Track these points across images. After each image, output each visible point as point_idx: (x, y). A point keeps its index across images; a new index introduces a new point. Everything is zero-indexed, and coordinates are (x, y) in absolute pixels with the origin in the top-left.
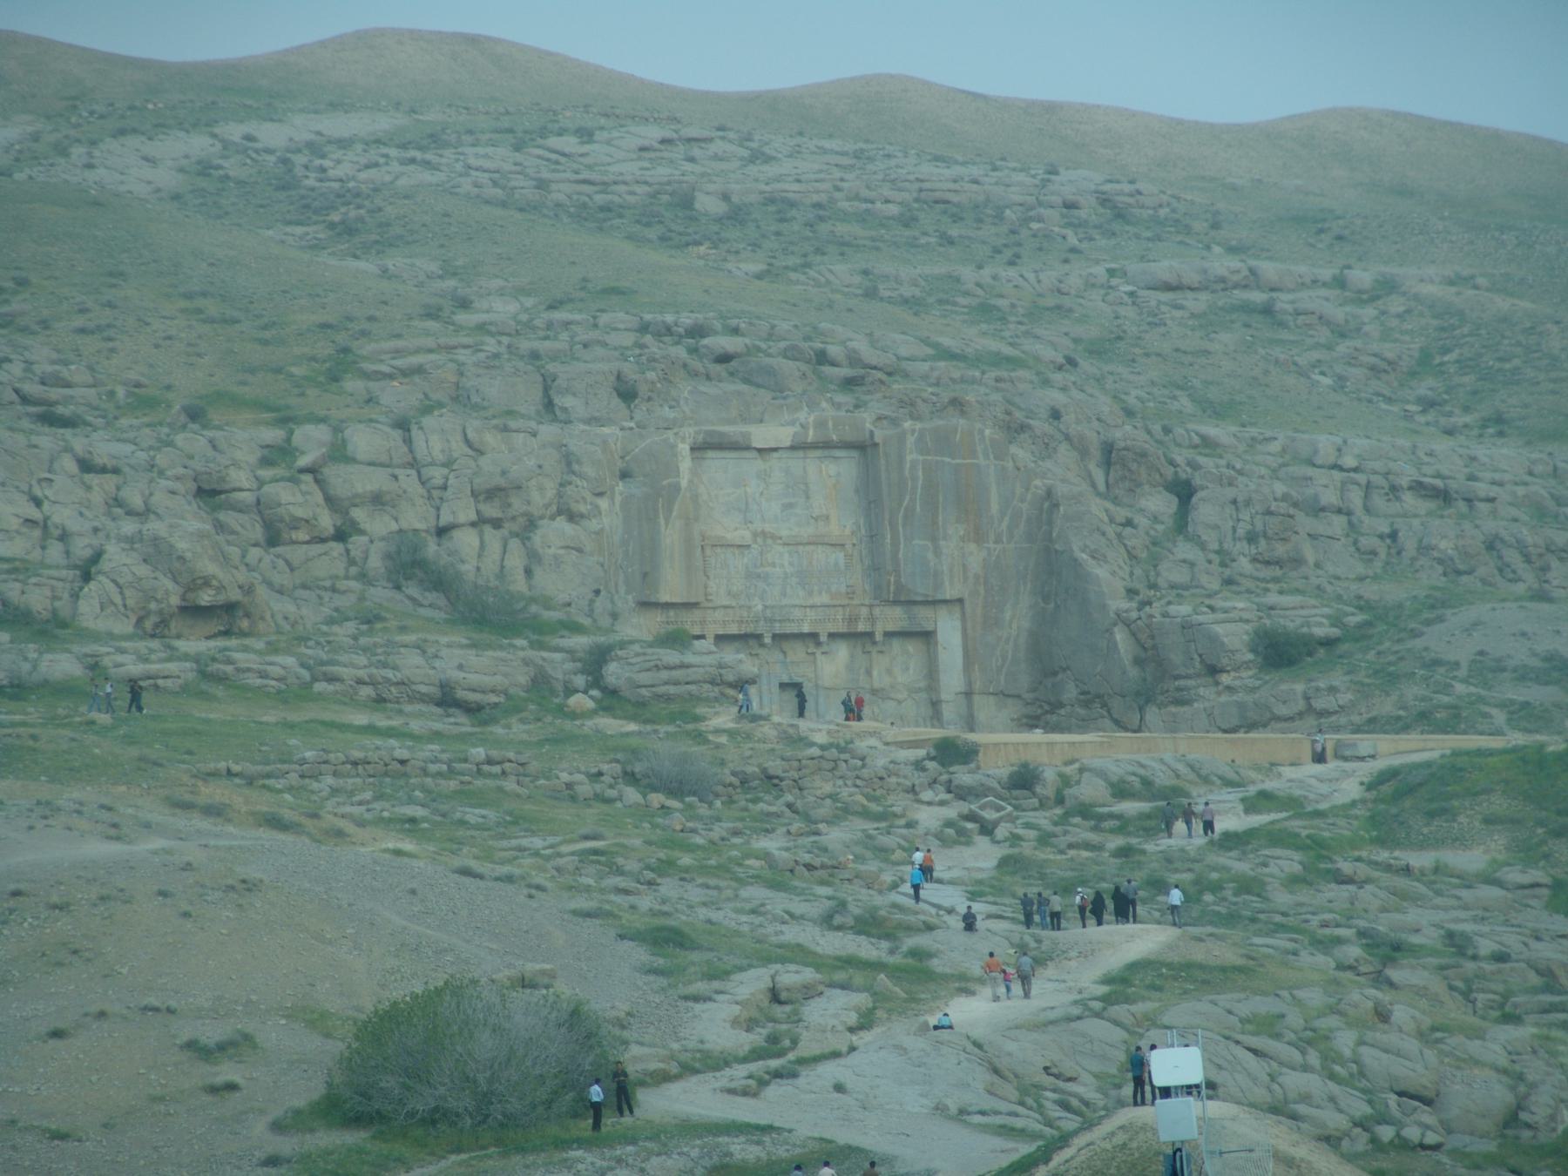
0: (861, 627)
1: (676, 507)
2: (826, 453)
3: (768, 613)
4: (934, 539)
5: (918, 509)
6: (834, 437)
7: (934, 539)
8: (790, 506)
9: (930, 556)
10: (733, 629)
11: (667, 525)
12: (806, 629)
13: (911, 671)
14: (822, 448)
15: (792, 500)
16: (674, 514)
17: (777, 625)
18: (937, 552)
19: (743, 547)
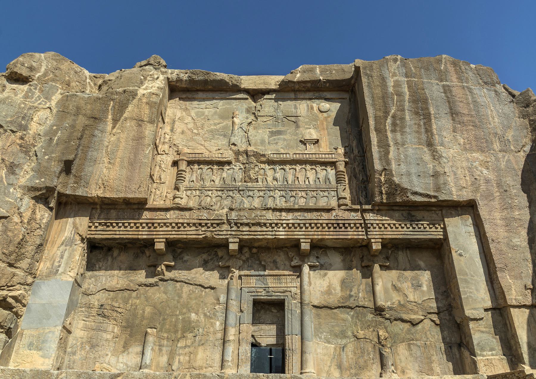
0: (352, 234)
1: (130, 108)
2: (317, 94)
3: (234, 215)
4: (430, 144)
5: (407, 118)
6: (321, 78)
7: (430, 144)
8: (279, 133)
9: (427, 157)
10: (191, 233)
11: (115, 121)
12: (282, 234)
13: (425, 288)
14: (308, 90)
15: (280, 128)
16: (125, 115)
17: (246, 228)
18: (436, 156)
19: (221, 164)
